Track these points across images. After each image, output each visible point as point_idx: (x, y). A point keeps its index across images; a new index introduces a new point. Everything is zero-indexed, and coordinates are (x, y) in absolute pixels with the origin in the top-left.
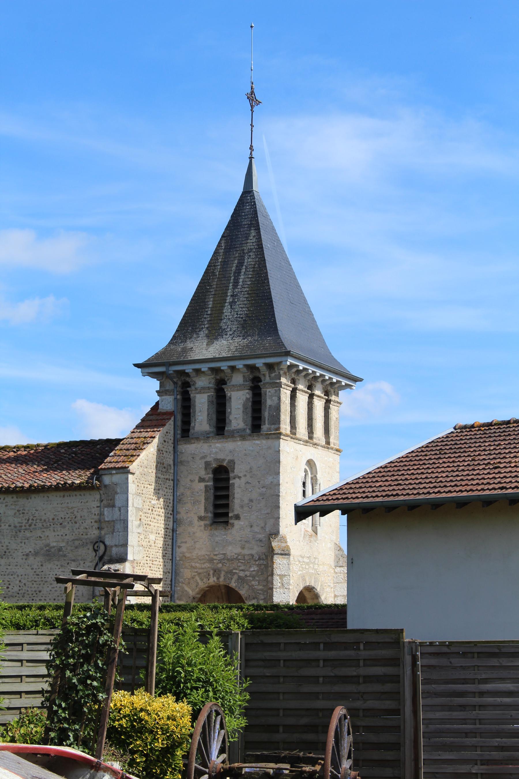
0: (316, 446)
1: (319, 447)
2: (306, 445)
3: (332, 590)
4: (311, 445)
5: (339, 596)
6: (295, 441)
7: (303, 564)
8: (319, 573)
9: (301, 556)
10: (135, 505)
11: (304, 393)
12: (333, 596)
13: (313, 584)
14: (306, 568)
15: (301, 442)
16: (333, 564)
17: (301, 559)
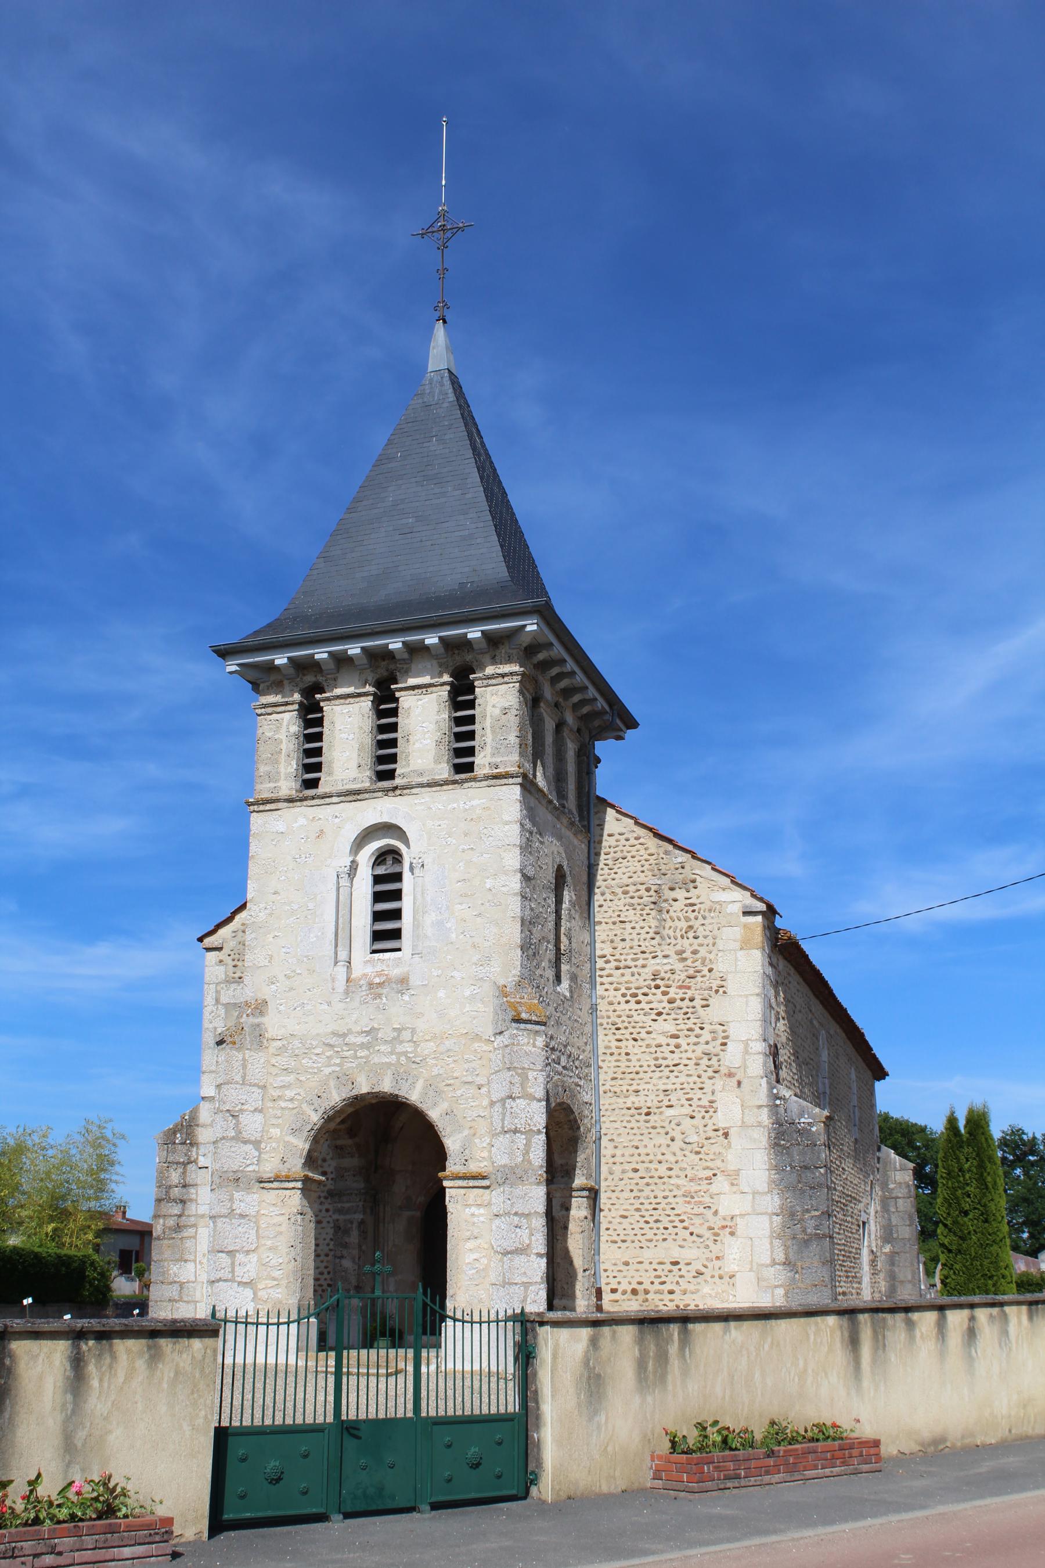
0: (398, 792)
1: (414, 791)
2: (360, 800)
3: (484, 1090)
4: (380, 794)
5: (495, 1102)
6: (305, 803)
7: (343, 1051)
8: (418, 1060)
9: (334, 1034)
10: (224, 999)
11: (351, 700)
12: (485, 1103)
13: (386, 1086)
14: (356, 1057)
15: (335, 799)
16: (488, 1031)
17: (333, 1041)
